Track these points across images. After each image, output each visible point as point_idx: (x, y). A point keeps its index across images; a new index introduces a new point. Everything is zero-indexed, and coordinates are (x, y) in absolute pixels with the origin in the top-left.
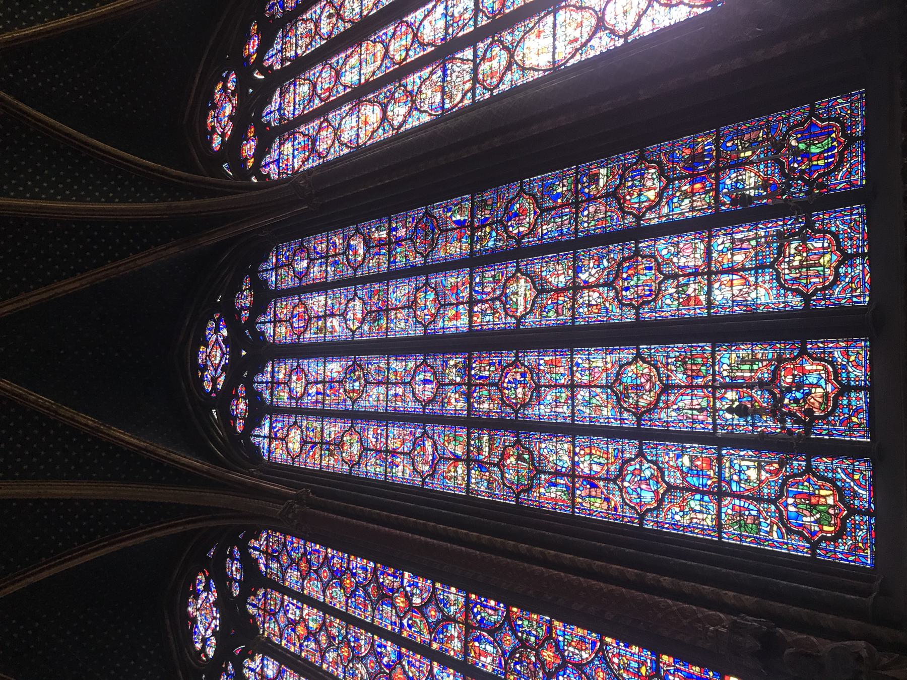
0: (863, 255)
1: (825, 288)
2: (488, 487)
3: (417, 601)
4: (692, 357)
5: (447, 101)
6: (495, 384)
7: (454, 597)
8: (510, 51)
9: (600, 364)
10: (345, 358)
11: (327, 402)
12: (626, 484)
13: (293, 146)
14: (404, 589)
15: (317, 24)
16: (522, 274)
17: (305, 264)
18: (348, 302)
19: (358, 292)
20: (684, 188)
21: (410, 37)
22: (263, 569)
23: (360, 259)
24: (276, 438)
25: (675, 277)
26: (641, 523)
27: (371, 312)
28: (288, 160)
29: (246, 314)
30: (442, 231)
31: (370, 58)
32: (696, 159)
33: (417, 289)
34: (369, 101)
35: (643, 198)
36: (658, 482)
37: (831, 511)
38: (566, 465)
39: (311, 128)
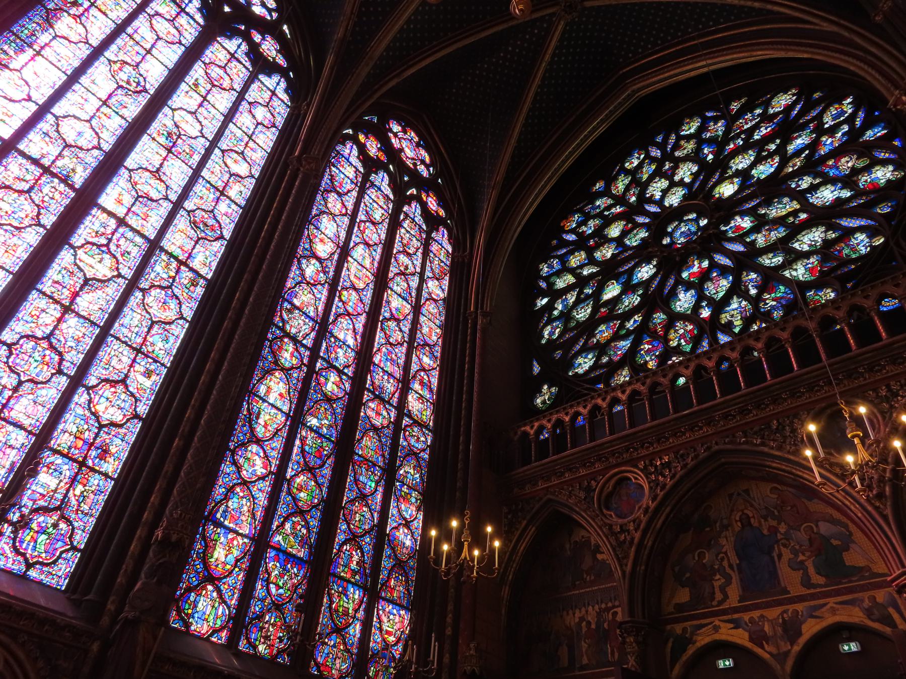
8: (285, 370)
15: (409, 255)
16: (114, 277)
19: (202, 140)
20: (87, 433)
21: (351, 310)
23: (229, 162)
29: (257, 38)
30: (199, 239)
31: (360, 274)
32: (104, 453)
34: (333, 253)
35: (103, 400)
39: (350, 201)
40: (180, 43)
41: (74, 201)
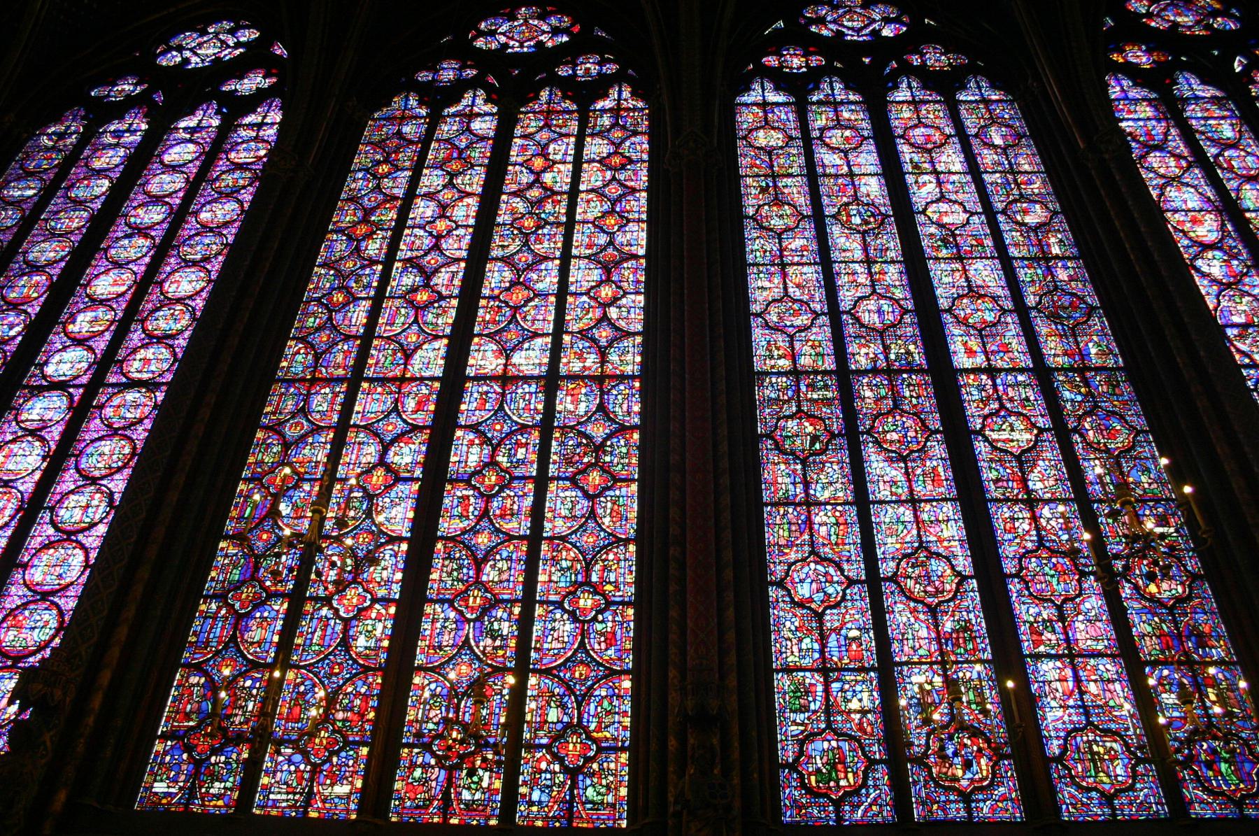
0: (1114, 815)
1: (1072, 777)
2: (770, 399)
3: (613, 313)
4: (973, 639)
5: (1235, 331)
6: (896, 406)
7: (628, 359)
9: (946, 534)
10: (888, 202)
11: (827, 181)
12: (812, 566)
13: (1149, 119)
14: (623, 296)
16: (1037, 436)
17: (998, 141)
18: (961, 204)
19: (975, 217)
22: (598, 106)
24: (766, 113)
25: (1062, 618)
26: (772, 583)
27: (954, 236)
28: (1129, 112)
30: (1072, 329)
33: (995, 299)
34: (1223, 225)
36: (822, 602)
37: (832, 784)
38: (818, 494)
39: (1176, 143)
40: (864, 138)
41: (935, 383)
